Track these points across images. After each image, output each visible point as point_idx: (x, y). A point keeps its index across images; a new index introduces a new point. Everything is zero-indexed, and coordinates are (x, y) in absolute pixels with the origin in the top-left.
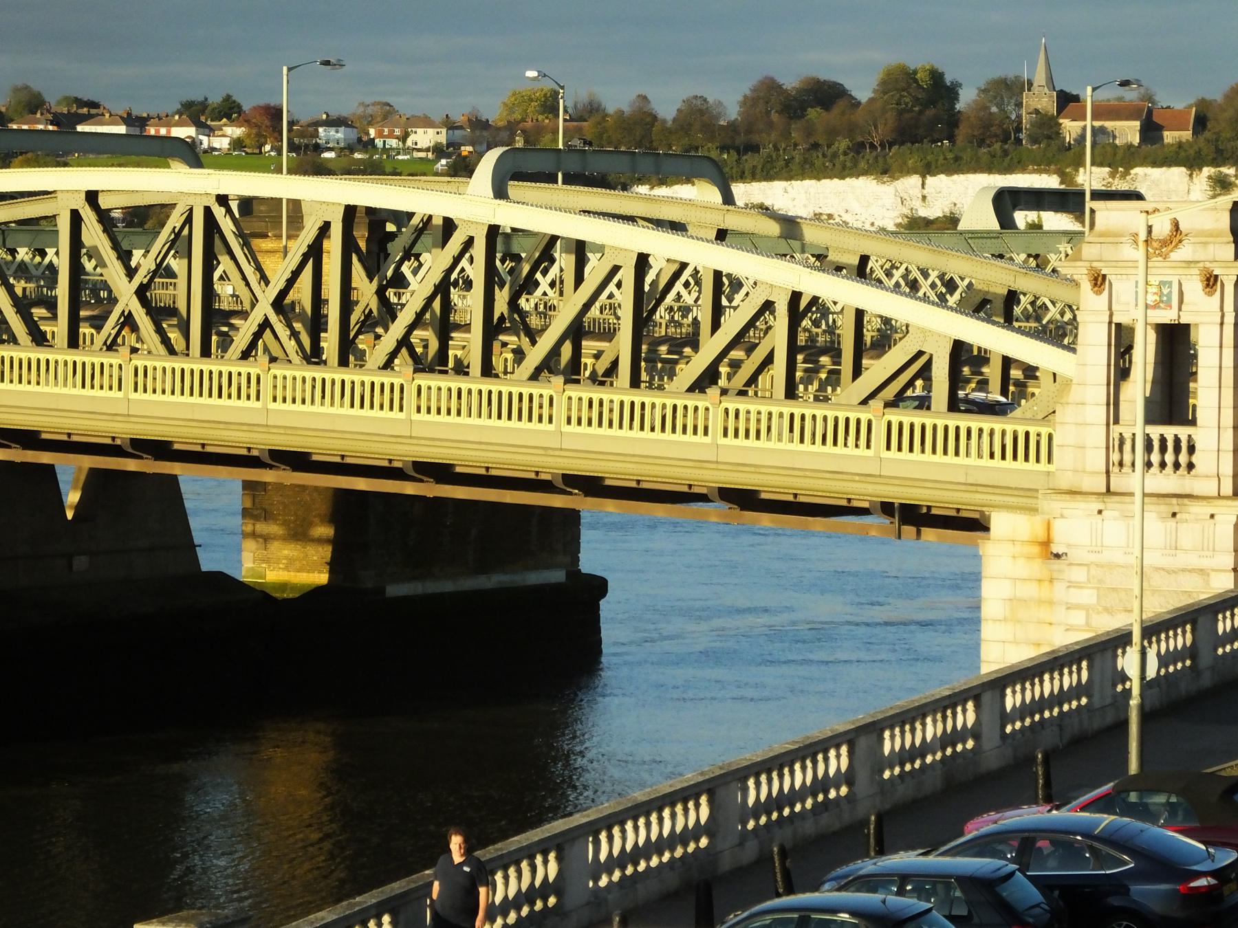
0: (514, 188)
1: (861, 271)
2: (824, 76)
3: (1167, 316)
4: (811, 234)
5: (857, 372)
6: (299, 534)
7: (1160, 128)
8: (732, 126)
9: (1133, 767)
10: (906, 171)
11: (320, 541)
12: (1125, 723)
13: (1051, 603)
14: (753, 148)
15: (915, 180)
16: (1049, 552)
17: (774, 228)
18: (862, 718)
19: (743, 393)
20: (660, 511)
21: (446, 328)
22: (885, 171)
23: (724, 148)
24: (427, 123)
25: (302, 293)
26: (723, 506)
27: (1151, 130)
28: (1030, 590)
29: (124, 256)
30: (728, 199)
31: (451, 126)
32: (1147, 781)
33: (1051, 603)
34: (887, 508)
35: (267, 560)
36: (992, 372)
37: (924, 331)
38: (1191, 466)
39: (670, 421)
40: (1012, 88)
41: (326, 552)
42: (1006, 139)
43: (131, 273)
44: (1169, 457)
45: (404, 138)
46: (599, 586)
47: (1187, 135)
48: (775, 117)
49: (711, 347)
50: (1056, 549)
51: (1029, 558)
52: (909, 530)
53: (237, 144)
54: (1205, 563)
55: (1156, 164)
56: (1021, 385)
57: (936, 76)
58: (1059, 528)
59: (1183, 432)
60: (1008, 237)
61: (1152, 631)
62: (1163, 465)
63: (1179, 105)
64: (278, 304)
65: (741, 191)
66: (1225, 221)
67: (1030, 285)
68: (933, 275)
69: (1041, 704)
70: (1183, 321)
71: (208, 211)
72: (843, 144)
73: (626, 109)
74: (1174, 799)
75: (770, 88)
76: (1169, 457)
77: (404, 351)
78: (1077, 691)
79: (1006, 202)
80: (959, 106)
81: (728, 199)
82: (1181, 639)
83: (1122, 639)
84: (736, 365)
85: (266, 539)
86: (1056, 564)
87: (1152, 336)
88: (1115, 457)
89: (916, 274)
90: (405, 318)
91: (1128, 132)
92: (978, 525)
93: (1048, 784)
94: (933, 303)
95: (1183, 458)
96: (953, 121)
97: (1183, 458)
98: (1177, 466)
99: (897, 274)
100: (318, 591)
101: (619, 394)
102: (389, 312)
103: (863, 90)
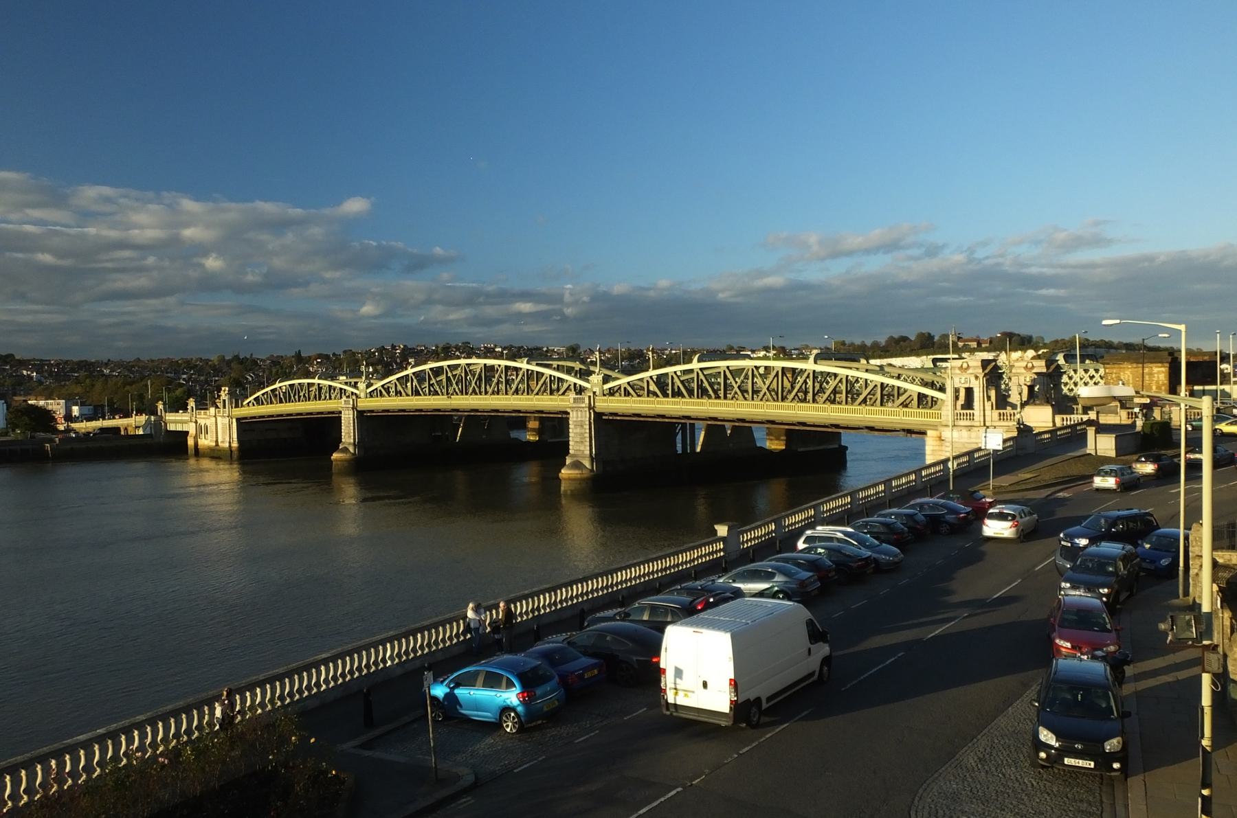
0: (818, 362)
1: (899, 377)
2: (904, 335)
3: (967, 386)
4: (886, 369)
5: (898, 398)
6: (778, 439)
7: (981, 344)
8: (883, 347)
9: (951, 488)
10: (923, 355)
11: (782, 440)
12: (949, 480)
13: (942, 451)
14: (888, 351)
15: (925, 357)
16: (940, 439)
17: (878, 369)
18: (888, 478)
19: (872, 405)
20: (852, 431)
21: (806, 393)
22: (918, 355)
23: (882, 351)
24: (816, 349)
25: (774, 385)
26: (866, 430)
27: (979, 344)
28: (937, 448)
29: (734, 379)
30: (868, 362)
31: (821, 349)
32: (953, 492)
33: (942, 451)
34: (904, 430)
35: (773, 444)
36: (929, 399)
37: (911, 390)
38: (973, 419)
39: (854, 411)
40: (946, 336)
41: (785, 442)
42: (946, 347)
43: (736, 382)
44: (962, 417)
45: (810, 352)
46: (846, 448)
47: (988, 345)
48: (893, 344)
49: (865, 393)
50: (943, 438)
51: (936, 440)
52: (909, 435)
53: (774, 355)
54: (977, 441)
55: (981, 352)
56: (936, 402)
57: (929, 334)
58: (943, 433)
59: (971, 412)
60: (936, 369)
61: (955, 458)
62: (967, 419)
63: (985, 339)
64: (768, 389)
65: (872, 362)
66: (980, 364)
67: (936, 379)
68: (911, 378)
69: (931, 474)
70: (971, 386)
71: (752, 370)
72: (909, 349)
73: (859, 343)
74: (958, 496)
75: (892, 338)
76: (968, 417)
77: (796, 397)
78: (940, 471)
79: (935, 361)
80: (935, 340)
81: (868, 362)
82: (965, 459)
83: (947, 460)
84: (871, 399)
85: (771, 440)
86: (943, 442)
87: (964, 390)
88: (956, 418)
89: (914, 378)
90: (796, 390)
91: (974, 345)
92: (924, 433)
93: (931, 492)
94: (918, 385)
95: (971, 418)
96: (933, 343)
97: (971, 418)
98: (970, 419)
99: (911, 378)
100: (783, 450)
101: (844, 407)
102: (793, 388)
103: (913, 338)
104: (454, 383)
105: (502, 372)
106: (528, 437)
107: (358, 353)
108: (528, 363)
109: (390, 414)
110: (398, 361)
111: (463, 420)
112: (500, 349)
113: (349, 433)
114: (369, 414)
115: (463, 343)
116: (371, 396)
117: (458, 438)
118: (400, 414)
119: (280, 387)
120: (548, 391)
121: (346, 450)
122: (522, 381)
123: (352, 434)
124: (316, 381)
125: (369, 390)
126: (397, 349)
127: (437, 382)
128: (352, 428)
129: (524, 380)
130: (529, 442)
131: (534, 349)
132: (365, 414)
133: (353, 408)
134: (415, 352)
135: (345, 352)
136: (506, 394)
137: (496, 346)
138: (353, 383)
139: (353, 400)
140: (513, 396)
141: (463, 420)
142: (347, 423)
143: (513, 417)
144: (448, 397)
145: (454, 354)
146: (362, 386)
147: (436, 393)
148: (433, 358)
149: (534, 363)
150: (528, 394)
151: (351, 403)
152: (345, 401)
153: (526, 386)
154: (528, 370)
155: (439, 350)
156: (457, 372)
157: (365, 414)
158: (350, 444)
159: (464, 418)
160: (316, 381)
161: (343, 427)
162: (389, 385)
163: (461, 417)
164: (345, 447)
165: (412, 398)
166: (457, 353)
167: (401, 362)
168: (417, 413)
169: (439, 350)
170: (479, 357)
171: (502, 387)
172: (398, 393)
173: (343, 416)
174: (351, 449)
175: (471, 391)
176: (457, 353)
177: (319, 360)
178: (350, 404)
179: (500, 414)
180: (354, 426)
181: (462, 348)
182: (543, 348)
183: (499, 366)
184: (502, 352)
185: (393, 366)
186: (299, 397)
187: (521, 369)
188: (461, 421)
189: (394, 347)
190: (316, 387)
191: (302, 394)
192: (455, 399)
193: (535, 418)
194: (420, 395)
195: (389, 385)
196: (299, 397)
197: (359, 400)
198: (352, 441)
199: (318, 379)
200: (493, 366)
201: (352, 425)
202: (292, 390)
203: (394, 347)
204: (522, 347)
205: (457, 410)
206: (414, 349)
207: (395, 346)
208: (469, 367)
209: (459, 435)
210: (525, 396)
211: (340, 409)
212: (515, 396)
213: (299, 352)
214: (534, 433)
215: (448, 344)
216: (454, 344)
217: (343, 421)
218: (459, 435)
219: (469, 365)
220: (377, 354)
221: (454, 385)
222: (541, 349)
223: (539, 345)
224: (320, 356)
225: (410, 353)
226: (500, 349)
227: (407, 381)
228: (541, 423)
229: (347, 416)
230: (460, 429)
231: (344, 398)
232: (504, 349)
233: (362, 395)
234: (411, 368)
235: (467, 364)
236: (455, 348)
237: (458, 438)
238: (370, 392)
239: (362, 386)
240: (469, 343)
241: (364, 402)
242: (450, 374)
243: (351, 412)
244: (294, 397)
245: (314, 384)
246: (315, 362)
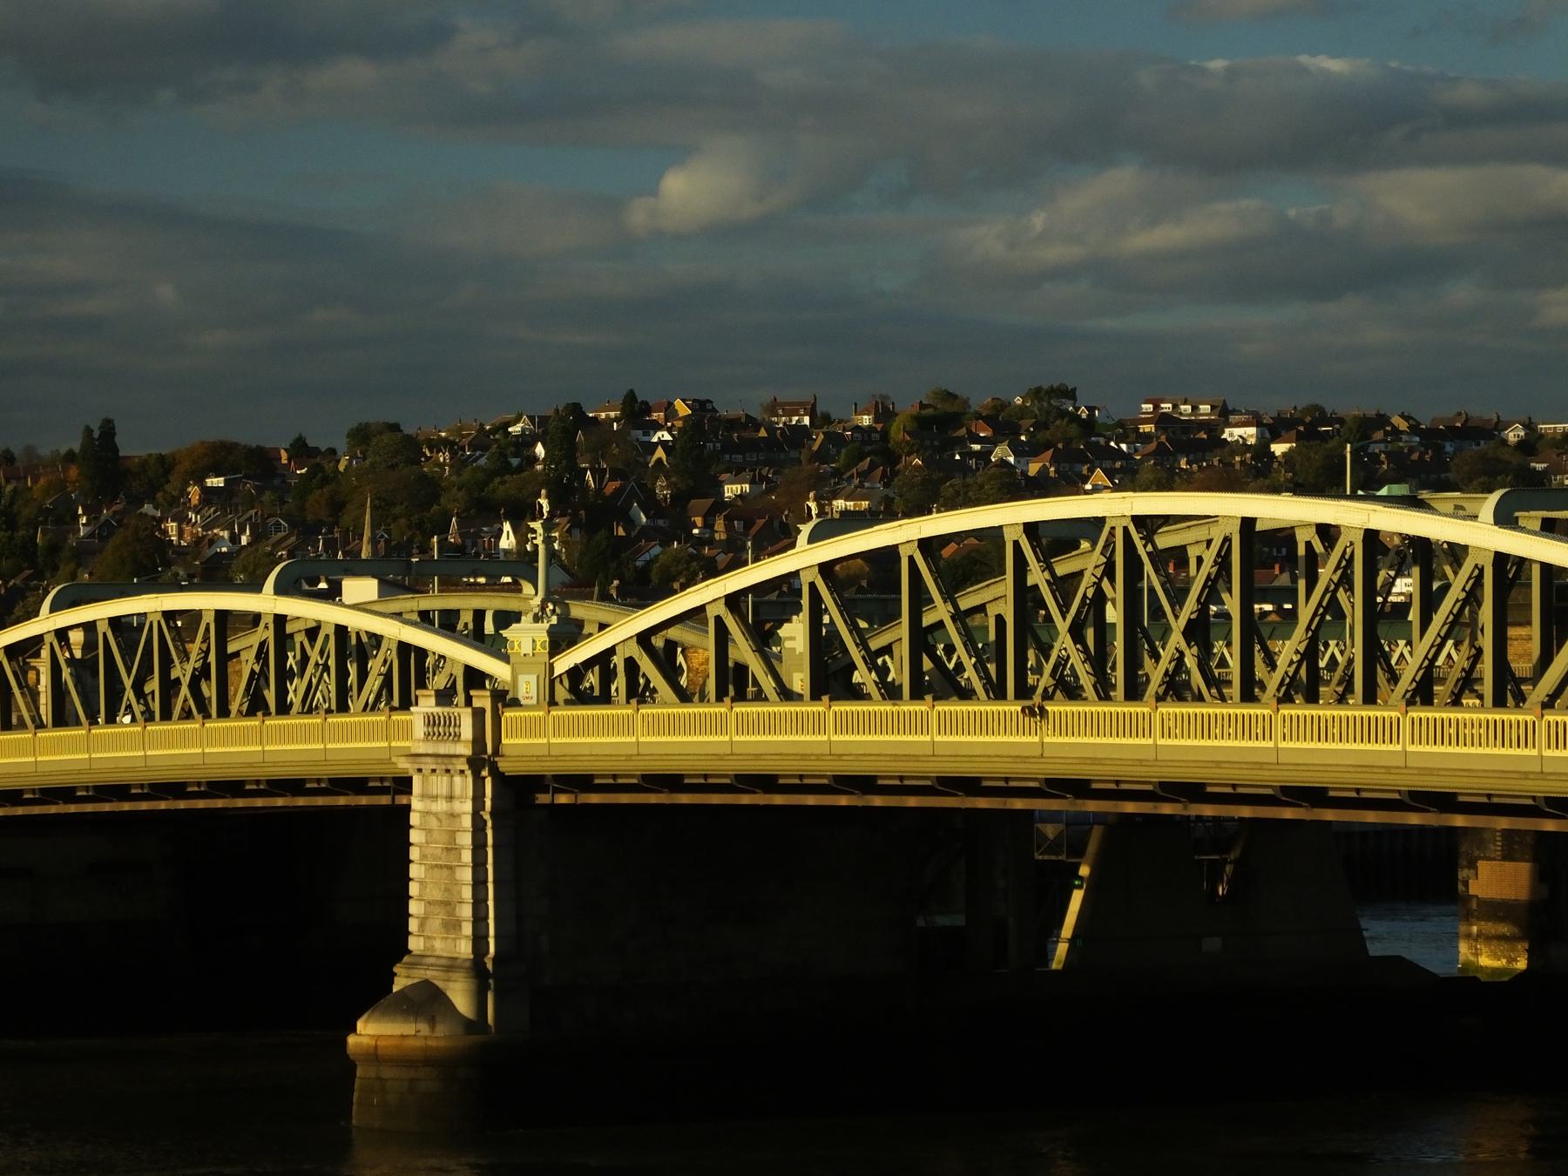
104: (1062, 626)
105: (1346, 580)
106: (1464, 949)
107: (436, 445)
108: (1504, 518)
109: (684, 799)
110: (662, 489)
111: (1092, 848)
112: (1250, 433)
113: (449, 905)
114: (563, 799)
115: (1036, 394)
116: (581, 697)
117: (1062, 949)
118: (746, 799)
119: (62, 634)
120: (1487, 688)
121: (428, 1001)
122: (1461, 626)
123: (466, 911)
124: (266, 602)
125: (564, 663)
126: (658, 427)
127: (959, 616)
128: (467, 875)
129: (1474, 627)
130: (1470, 985)
131: (1452, 433)
132: (543, 799)
133: (478, 762)
134: (755, 445)
135: (361, 436)
136: (1248, 696)
137: (1225, 414)
138: (467, 618)
139: (478, 715)
140: (1286, 711)
141: (1092, 848)
142: (437, 848)
143: (1409, 830)
144: (1029, 712)
145: (984, 456)
146: (527, 637)
147: (949, 686)
148: (864, 476)
149: (1533, 518)
150: (1370, 698)
151: (467, 731)
152: (431, 721)
153: (1358, 652)
154: (1501, 559)
155: (897, 432)
156: (1086, 561)
157: (543, 799)
158: (451, 965)
159: (1096, 833)
160: (266, 602)
161: (415, 871)
162: (674, 633)
163: (1081, 823)
164: (427, 985)
165: (721, 709)
166: (1002, 452)
167: (681, 499)
168: (843, 801)
169: (897, 432)
170: (1127, 478)
171: (1347, 649)
172: (734, 683)
173: (416, 804)
174: (460, 997)
175: (1155, 674)
176: (1002, 452)
177: (216, 482)
178: (457, 737)
179: (1329, 815)
180: (478, 865)
181: (1027, 423)
182: (1501, 425)
183: (1328, 533)
184: (1262, 451)
185: (629, 523)
186: (170, 687)
187: (1457, 553)
188: (1078, 850)
189: (637, 413)
190: (266, 633)
191: (182, 672)
192: (1063, 727)
193: (1512, 846)
194: (857, 694)
195: (674, 633)
196: (170, 687)
197: (508, 714)
198: (465, 949)
199: (280, 590)
200: (1283, 537)
201: (467, 856)
202: (128, 654)
203: (637, 413)
204: (1382, 420)
205: (1079, 787)
206: (753, 423)
207: (648, 410)
208: (1148, 539)
209: (1067, 930)
210: (1355, 711)
211: (404, 765)
212: (1299, 710)
213: (108, 430)
214: (1504, 929)
215: (950, 396)
216: (980, 400)
217: (415, 836)
218: (1067, 930)
219: (1146, 522)
220: (540, 450)
221: (1064, 643)
222: (1491, 431)
223: (1483, 411)
224: (220, 457)
225: (729, 447)
226: (1250, 433)
227: (788, 609)
228: (1542, 875)
229: (441, 806)
230: (1077, 897)
231: (426, 704)
232: (1273, 430)
233: (528, 688)
234: (813, 539)
235: (1139, 520)
236: (990, 420)
237: (1062, 949)
238: (576, 674)
239: (527, 637)
240: (1071, 394)
241: (532, 728)
242: (1037, 576)
243: (464, 785)
244: (138, 687)
245: (255, 619)
246: (194, 492)
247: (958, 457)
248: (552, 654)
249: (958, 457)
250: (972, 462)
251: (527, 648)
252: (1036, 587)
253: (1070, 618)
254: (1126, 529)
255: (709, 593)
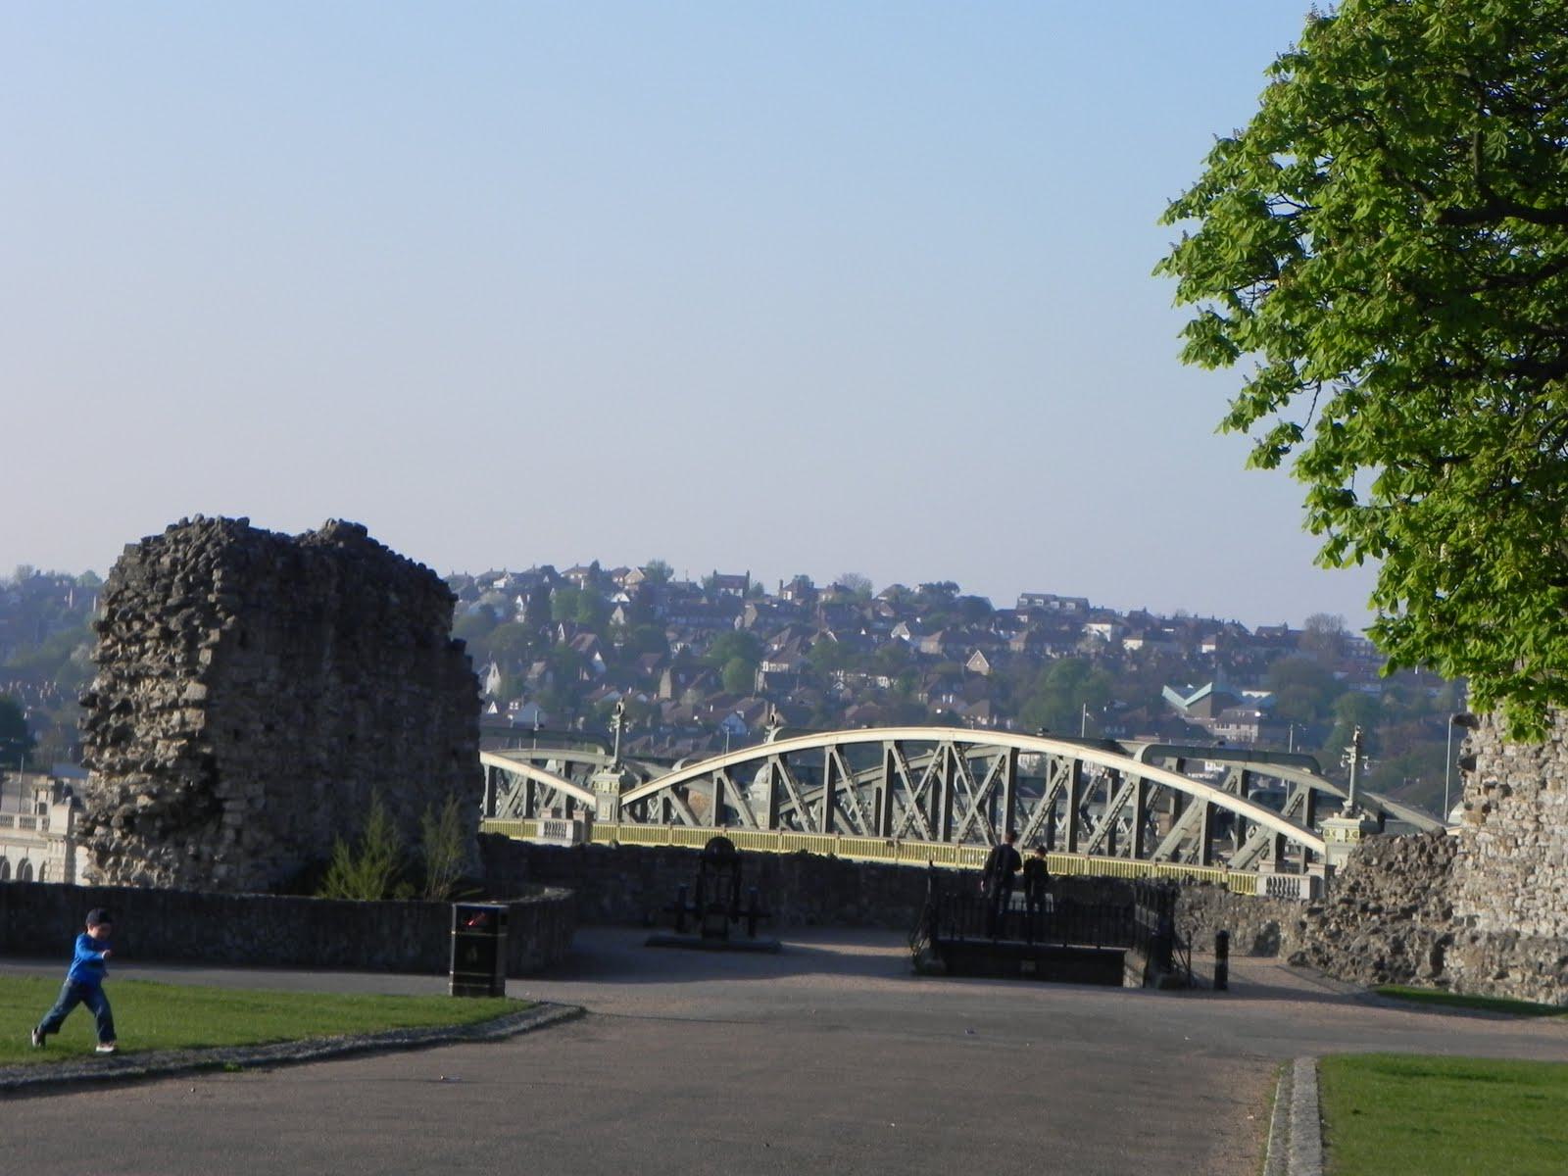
125: (628, 798)
139: (577, 825)
145: (887, 633)
156: (930, 761)
208: (961, 753)
234: (777, 738)
235: (957, 744)
238: (633, 804)
242: (899, 768)
247: (863, 632)
248: (621, 792)
249: (863, 632)
250: (875, 637)
251: (606, 787)
252: (899, 774)
253: (916, 794)
254: (950, 748)
255: (715, 764)
